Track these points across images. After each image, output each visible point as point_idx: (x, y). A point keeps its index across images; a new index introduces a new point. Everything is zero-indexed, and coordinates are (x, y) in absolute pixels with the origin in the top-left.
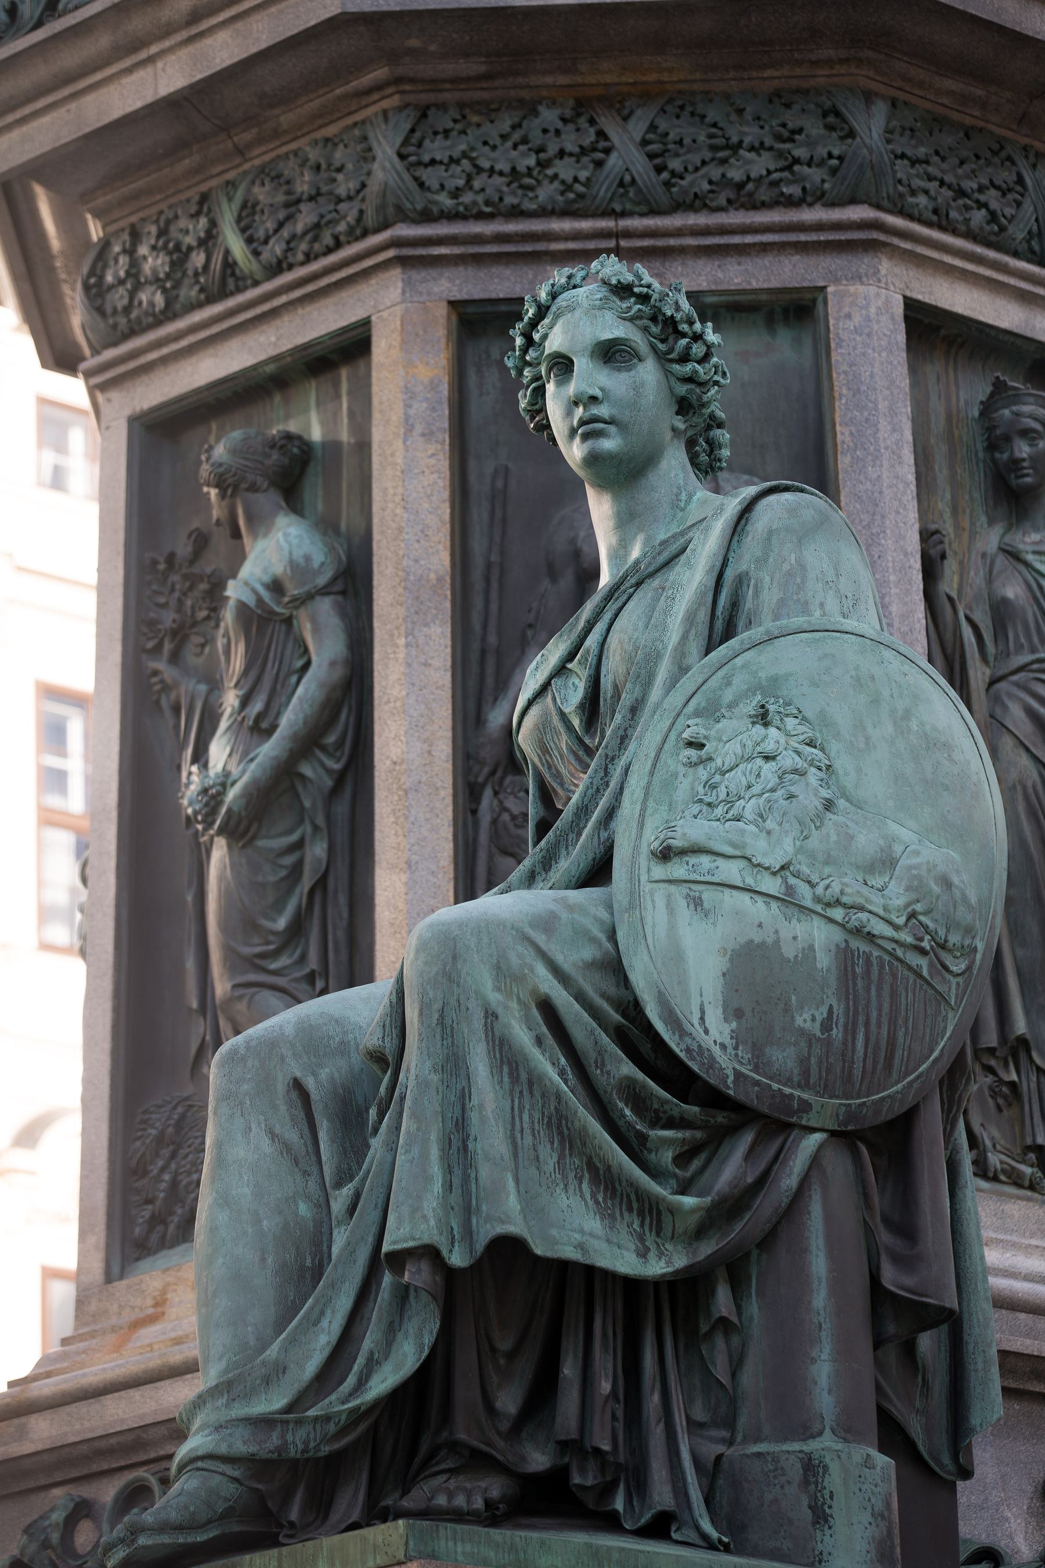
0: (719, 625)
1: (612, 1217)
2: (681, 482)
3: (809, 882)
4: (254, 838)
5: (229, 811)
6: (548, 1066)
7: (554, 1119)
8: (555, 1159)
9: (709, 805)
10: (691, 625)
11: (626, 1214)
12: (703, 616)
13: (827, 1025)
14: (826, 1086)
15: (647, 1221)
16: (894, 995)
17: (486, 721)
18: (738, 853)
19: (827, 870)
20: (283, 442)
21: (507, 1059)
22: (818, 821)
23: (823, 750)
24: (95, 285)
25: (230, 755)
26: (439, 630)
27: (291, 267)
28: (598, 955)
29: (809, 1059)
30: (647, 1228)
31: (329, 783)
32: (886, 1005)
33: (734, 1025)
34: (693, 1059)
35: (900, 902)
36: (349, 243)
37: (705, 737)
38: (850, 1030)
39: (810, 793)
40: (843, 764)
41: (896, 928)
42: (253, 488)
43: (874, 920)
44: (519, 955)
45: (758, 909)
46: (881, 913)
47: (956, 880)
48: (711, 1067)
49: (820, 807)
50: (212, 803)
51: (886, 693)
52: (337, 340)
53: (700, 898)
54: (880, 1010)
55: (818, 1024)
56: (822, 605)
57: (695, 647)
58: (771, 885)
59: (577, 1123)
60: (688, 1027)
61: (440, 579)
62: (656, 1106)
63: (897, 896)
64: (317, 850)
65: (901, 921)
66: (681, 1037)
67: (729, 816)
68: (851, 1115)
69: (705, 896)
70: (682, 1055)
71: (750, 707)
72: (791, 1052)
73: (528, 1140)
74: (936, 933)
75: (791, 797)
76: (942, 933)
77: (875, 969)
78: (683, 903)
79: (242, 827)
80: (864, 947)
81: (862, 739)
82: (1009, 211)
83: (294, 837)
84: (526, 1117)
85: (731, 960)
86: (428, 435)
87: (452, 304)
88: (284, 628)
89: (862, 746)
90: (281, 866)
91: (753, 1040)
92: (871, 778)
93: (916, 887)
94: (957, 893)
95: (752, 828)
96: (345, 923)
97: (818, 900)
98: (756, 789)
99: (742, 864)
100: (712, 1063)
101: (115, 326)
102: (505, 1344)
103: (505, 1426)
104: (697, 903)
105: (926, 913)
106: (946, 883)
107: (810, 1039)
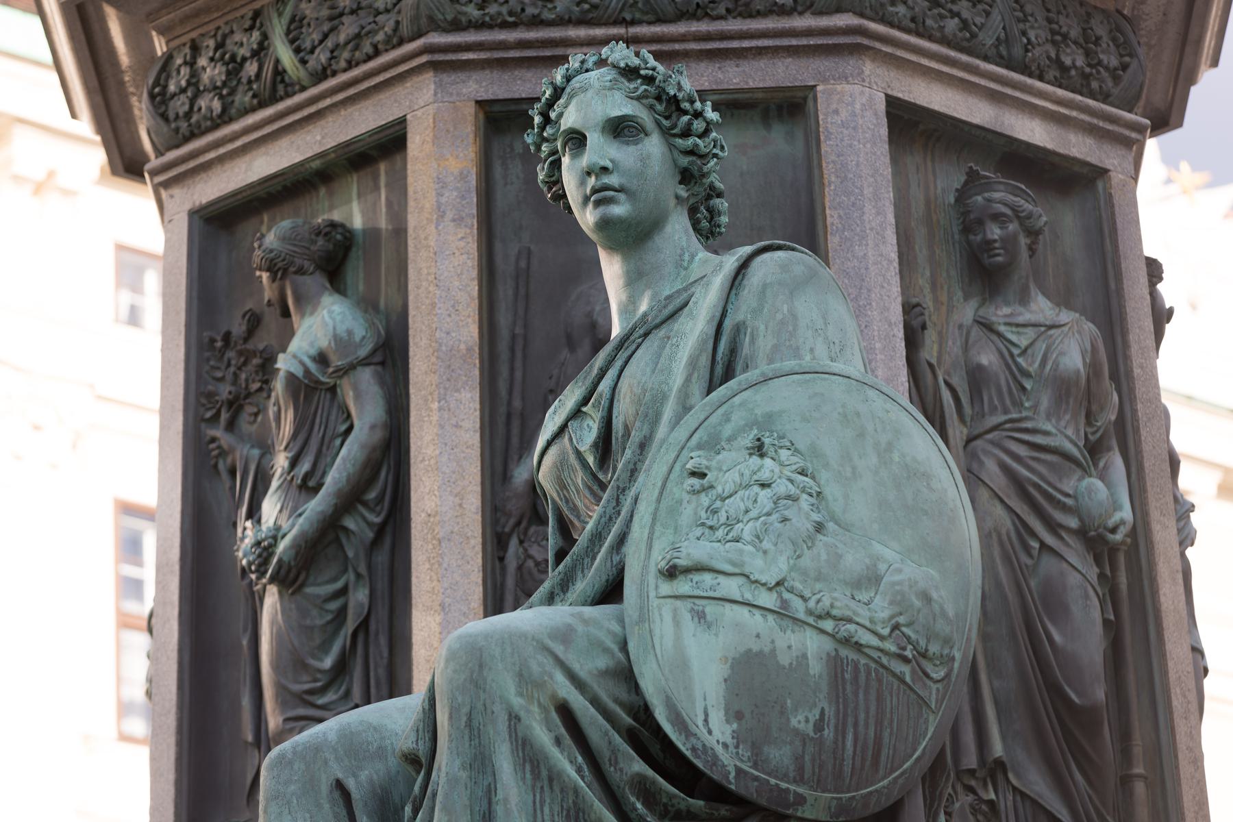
0: (719, 369)
2: (684, 244)
3: (802, 597)
4: (302, 585)
5: (280, 560)
6: (567, 763)
7: (572, 812)
9: (711, 528)
10: (694, 369)
12: (705, 360)
13: (819, 727)
14: (819, 781)
16: (880, 699)
17: (512, 477)
18: (737, 571)
19: (818, 586)
20: (327, 229)
21: (530, 759)
22: (810, 541)
23: (813, 478)
24: (159, 94)
25: (281, 511)
26: (469, 395)
27: (334, 74)
28: (611, 663)
29: (803, 757)
31: (370, 535)
32: (873, 709)
33: (735, 726)
34: (699, 757)
35: (885, 614)
36: (387, 50)
37: (707, 468)
38: (841, 731)
39: (802, 516)
40: (832, 491)
41: (882, 638)
42: (301, 271)
43: (861, 631)
44: (539, 664)
45: (756, 621)
46: (868, 624)
47: (935, 595)
48: (714, 764)
49: (811, 529)
50: (265, 554)
52: (376, 137)
53: (703, 612)
54: (867, 713)
55: (811, 725)
56: (812, 350)
57: (697, 388)
58: (768, 599)
59: (593, 816)
60: (693, 728)
61: (469, 350)
62: (664, 800)
63: (882, 609)
64: (360, 596)
65: (886, 632)
66: (687, 737)
67: (729, 537)
69: (708, 610)
70: (688, 754)
71: (747, 440)
72: (787, 750)
75: (785, 520)
76: (923, 643)
78: (688, 616)
79: (292, 575)
80: (852, 655)
81: (849, 469)
82: (979, 20)
83: (339, 584)
84: (547, 810)
85: (732, 667)
86: (458, 220)
87: (477, 102)
88: (328, 396)
89: (849, 474)
90: (327, 611)
91: (753, 738)
93: (899, 601)
94: (936, 607)
95: (750, 548)
96: (385, 661)
97: (810, 612)
98: (753, 514)
99: (741, 580)
101: (177, 130)
104: (700, 616)
105: (908, 625)
106: (926, 598)
107: (804, 739)
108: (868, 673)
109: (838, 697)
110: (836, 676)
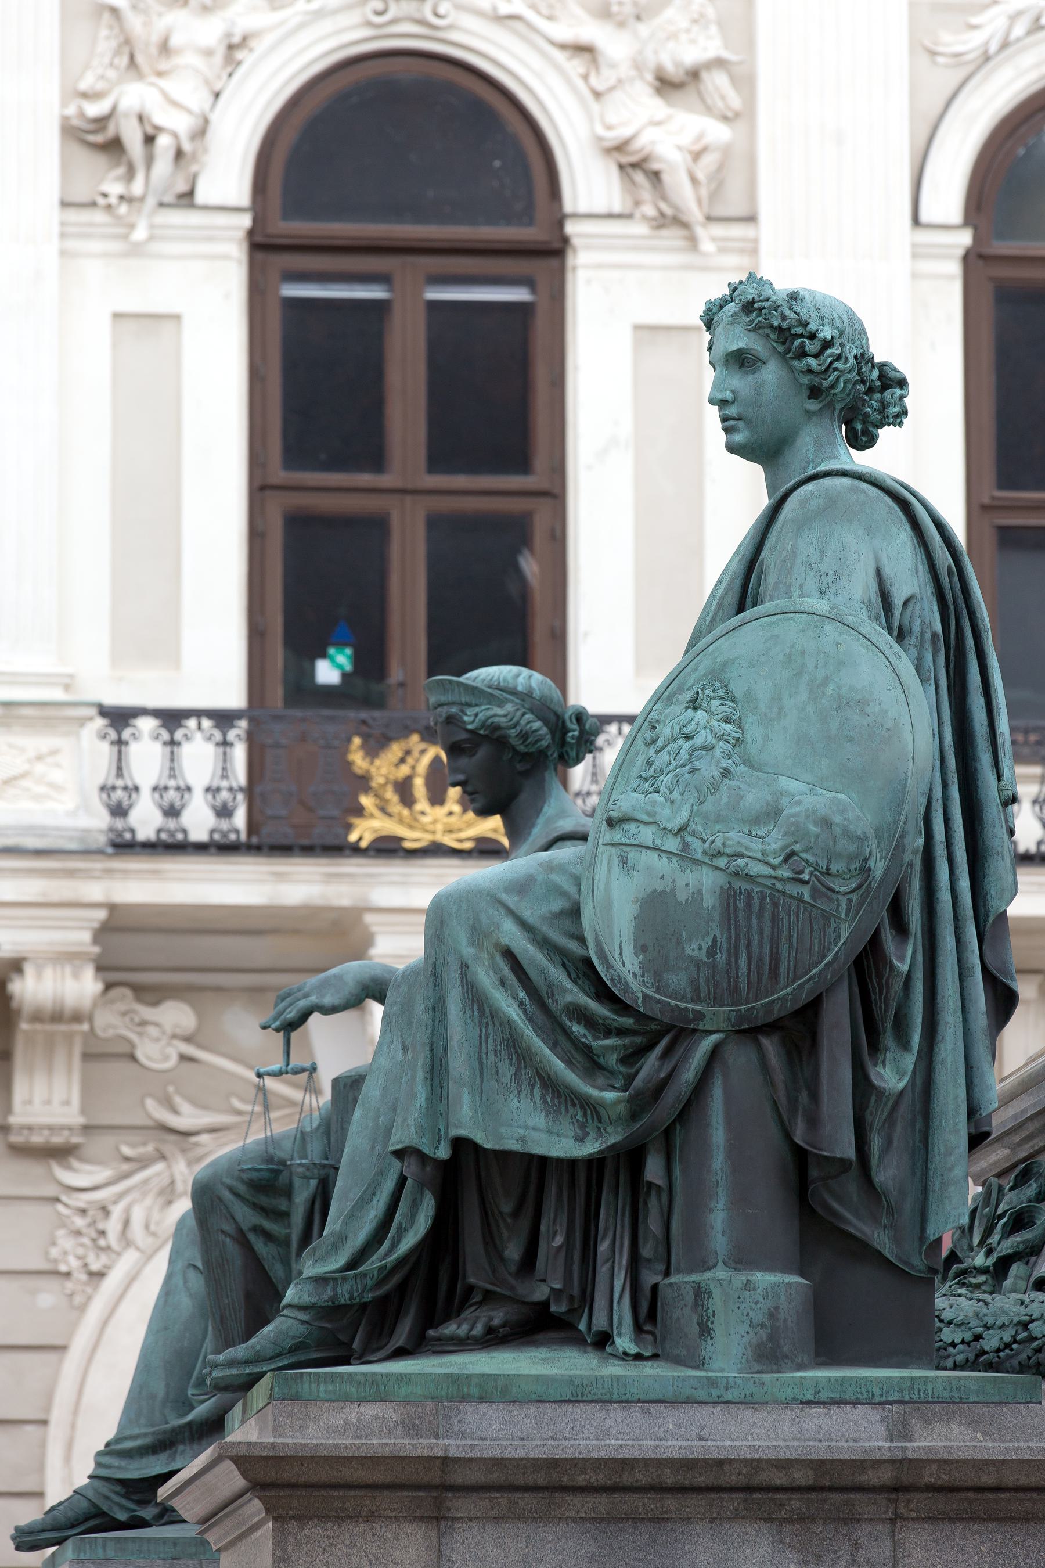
1: (558, 1112)
2: (811, 456)
3: (701, 839)
8: (513, 1071)
11: (571, 1109)
13: (712, 952)
14: (715, 998)
15: (589, 1112)
16: (775, 919)
19: (717, 827)
22: (715, 788)
23: (739, 725)
30: (589, 1117)
32: (767, 931)
33: (641, 957)
34: (615, 986)
38: (733, 953)
40: (754, 732)
43: (752, 864)
46: (760, 856)
48: (627, 991)
55: (704, 951)
56: (801, 585)
63: (775, 841)
68: (741, 1017)
72: (683, 975)
73: (492, 1059)
74: (817, 864)
76: (823, 864)
77: (756, 903)
81: (775, 710)
91: (655, 966)
92: (772, 743)
93: (796, 832)
94: (838, 831)
95: (662, 799)
99: (652, 829)
100: (627, 988)
102: (507, 1208)
103: (513, 1268)
105: (806, 850)
107: (698, 964)
108: (763, 898)
109: (730, 924)
110: (728, 905)
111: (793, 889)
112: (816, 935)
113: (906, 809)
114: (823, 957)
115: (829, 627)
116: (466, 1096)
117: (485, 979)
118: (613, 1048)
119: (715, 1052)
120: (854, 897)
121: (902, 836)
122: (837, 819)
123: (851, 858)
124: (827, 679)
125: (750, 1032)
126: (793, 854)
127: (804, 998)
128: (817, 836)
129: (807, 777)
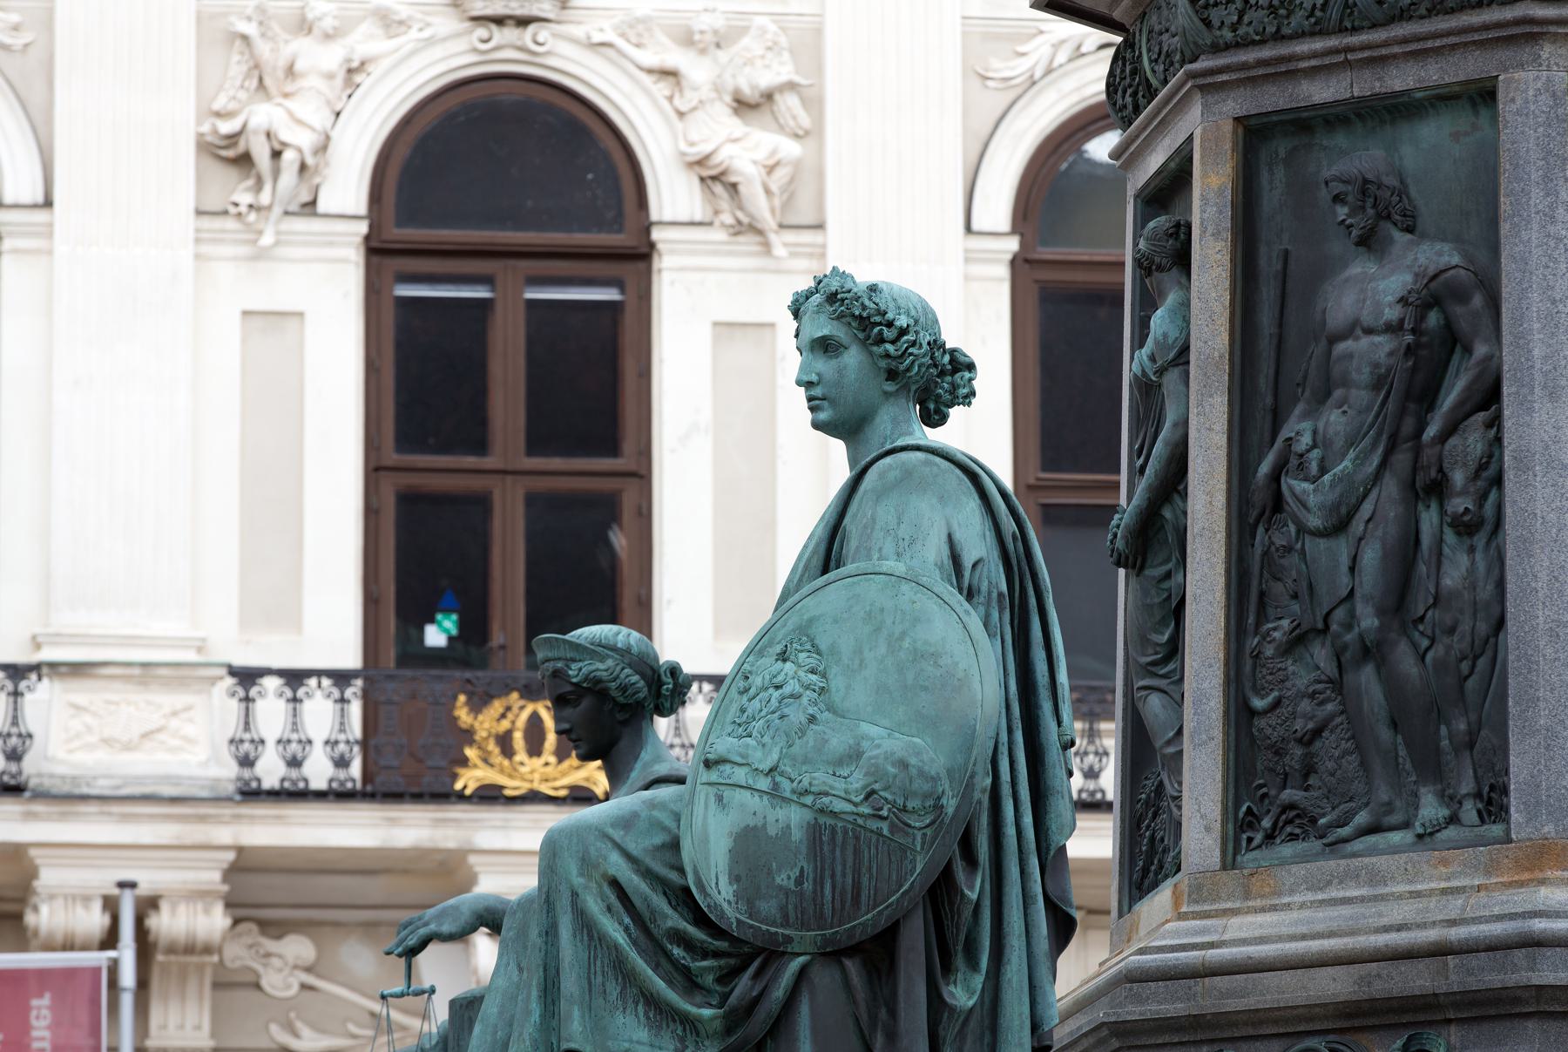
1: (660, 1028)
13: (799, 881)
16: (857, 852)
19: (804, 768)
22: (802, 732)
23: (824, 676)
38: (819, 882)
40: (837, 683)
41: (856, 805)
49: (804, 720)
51: (889, 622)
65: (858, 800)
72: (774, 902)
73: (600, 979)
76: (900, 802)
80: (830, 821)
81: (857, 662)
84: (598, 963)
92: (853, 691)
93: (875, 772)
94: (914, 771)
97: (794, 792)
100: (722, 914)
105: (885, 789)
107: (787, 892)
111: (874, 825)
112: (894, 866)
113: (975, 752)
114: (901, 886)
115: (905, 587)
116: (576, 1013)
117: (593, 906)
118: (710, 969)
119: (803, 972)
120: (929, 832)
121: (972, 777)
122: (913, 761)
123: (926, 796)
124: (904, 634)
125: (834, 954)
126: (873, 792)
127: (883, 923)
128: (895, 777)
129: (886, 722)
